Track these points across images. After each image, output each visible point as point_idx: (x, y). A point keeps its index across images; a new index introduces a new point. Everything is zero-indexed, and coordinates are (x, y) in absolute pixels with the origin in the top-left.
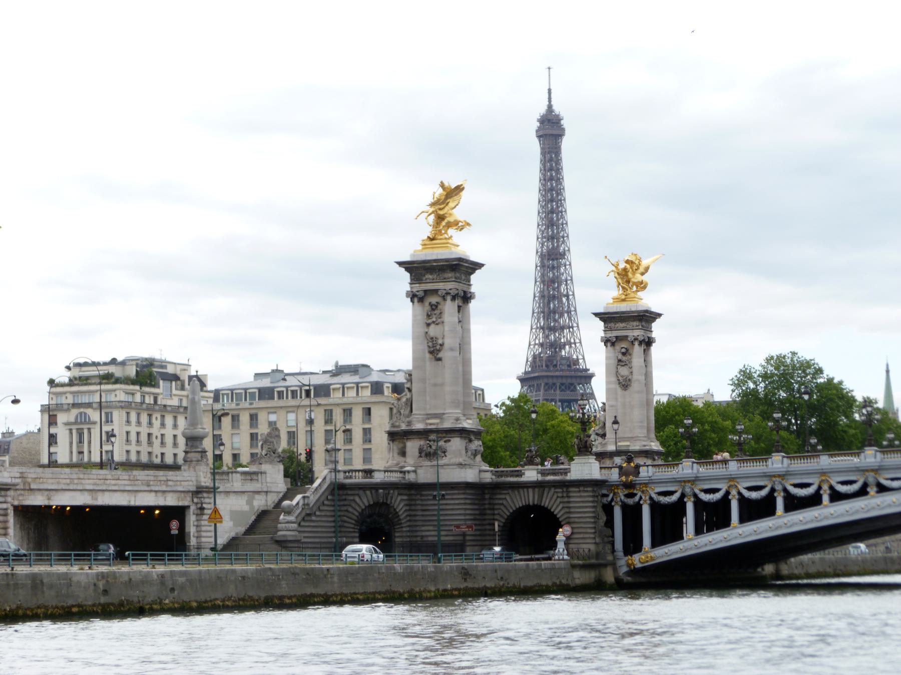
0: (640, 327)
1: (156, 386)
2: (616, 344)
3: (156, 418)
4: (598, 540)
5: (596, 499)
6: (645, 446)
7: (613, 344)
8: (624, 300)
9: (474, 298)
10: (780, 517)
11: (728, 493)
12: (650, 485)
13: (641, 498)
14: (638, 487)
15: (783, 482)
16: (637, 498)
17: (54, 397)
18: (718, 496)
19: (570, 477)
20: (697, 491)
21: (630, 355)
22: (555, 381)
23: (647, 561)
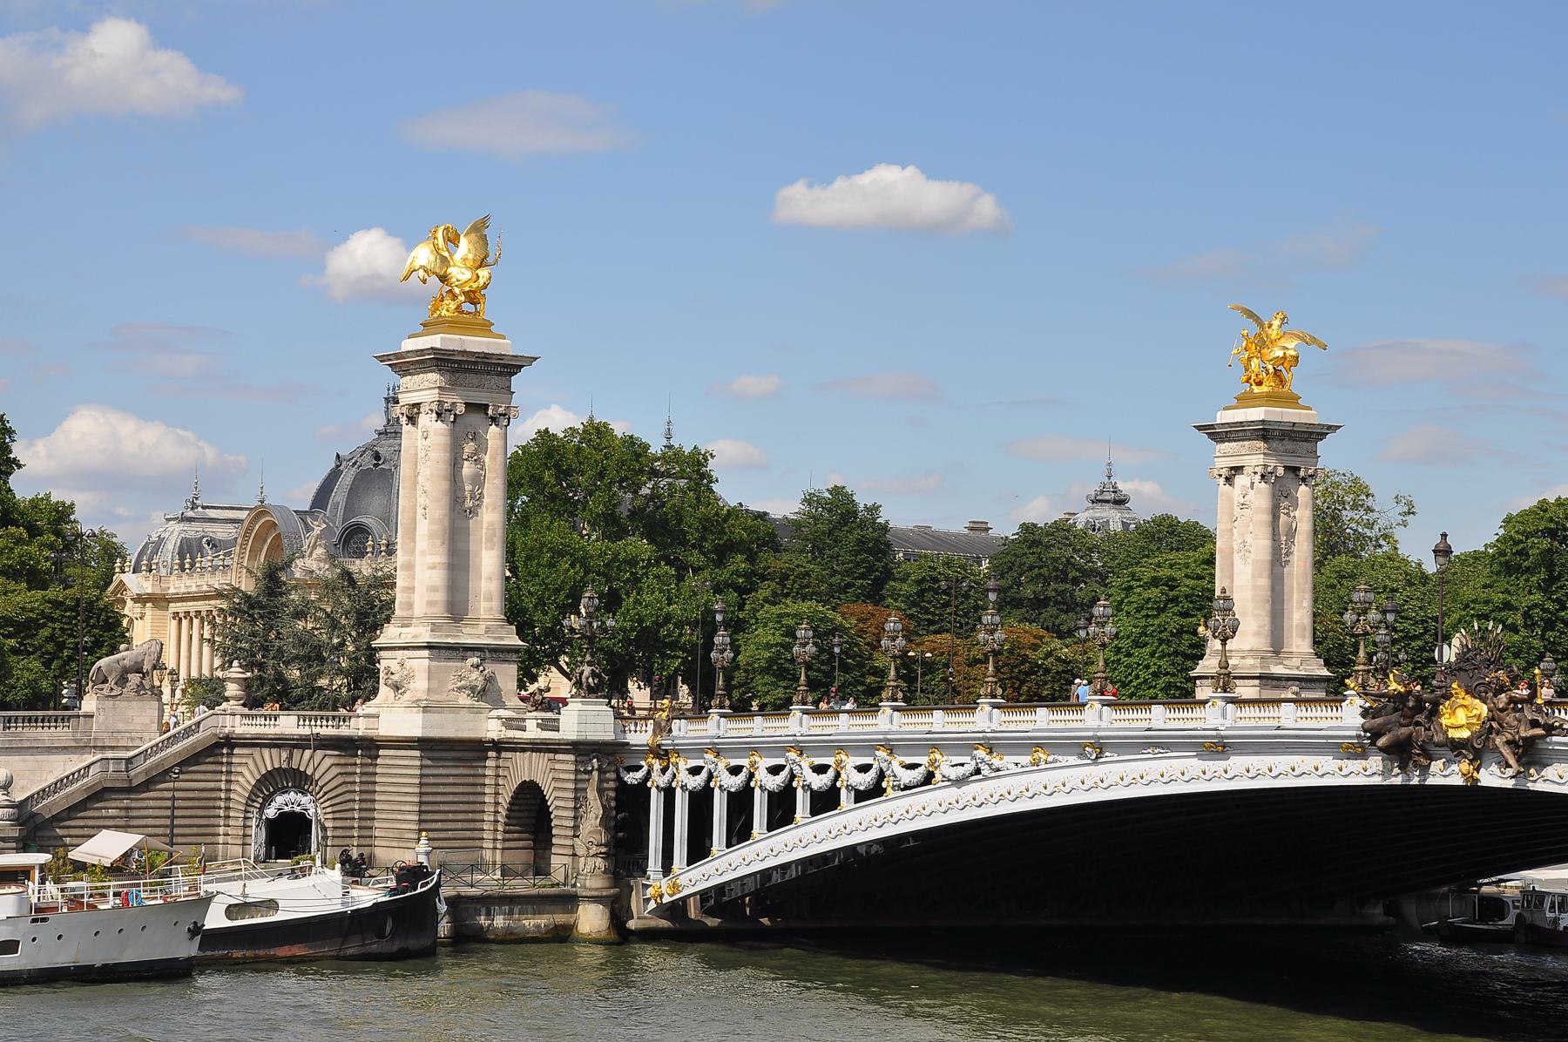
5: (587, 777)
16: (669, 774)
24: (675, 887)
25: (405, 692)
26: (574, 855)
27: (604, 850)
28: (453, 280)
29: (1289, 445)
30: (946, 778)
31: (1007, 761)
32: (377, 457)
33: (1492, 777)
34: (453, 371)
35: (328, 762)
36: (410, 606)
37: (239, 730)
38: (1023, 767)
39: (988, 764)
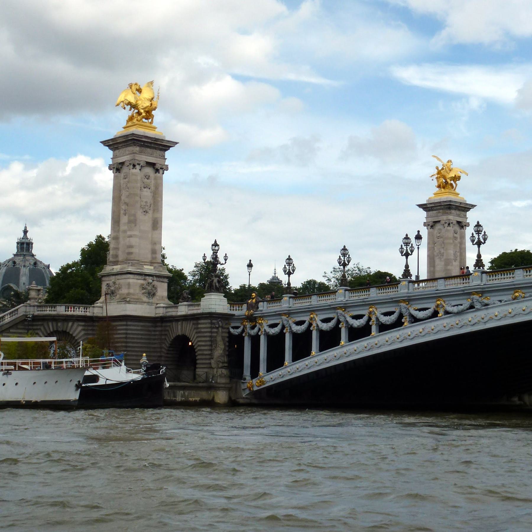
5: (215, 330)
9: (167, 169)
11: (310, 325)
12: (265, 319)
13: (259, 330)
15: (343, 313)
16: (256, 329)
18: (303, 327)
23: (261, 386)
24: (263, 383)
25: (116, 295)
26: (211, 368)
27: (226, 365)
28: (141, 106)
29: (458, 212)
30: (447, 313)
31: (493, 299)
32: (14, 263)
34: (141, 146)
35: (80, 328)
36: (116, 256)
37: (36, 313)
38: (506, 301)
39: (480, 302)
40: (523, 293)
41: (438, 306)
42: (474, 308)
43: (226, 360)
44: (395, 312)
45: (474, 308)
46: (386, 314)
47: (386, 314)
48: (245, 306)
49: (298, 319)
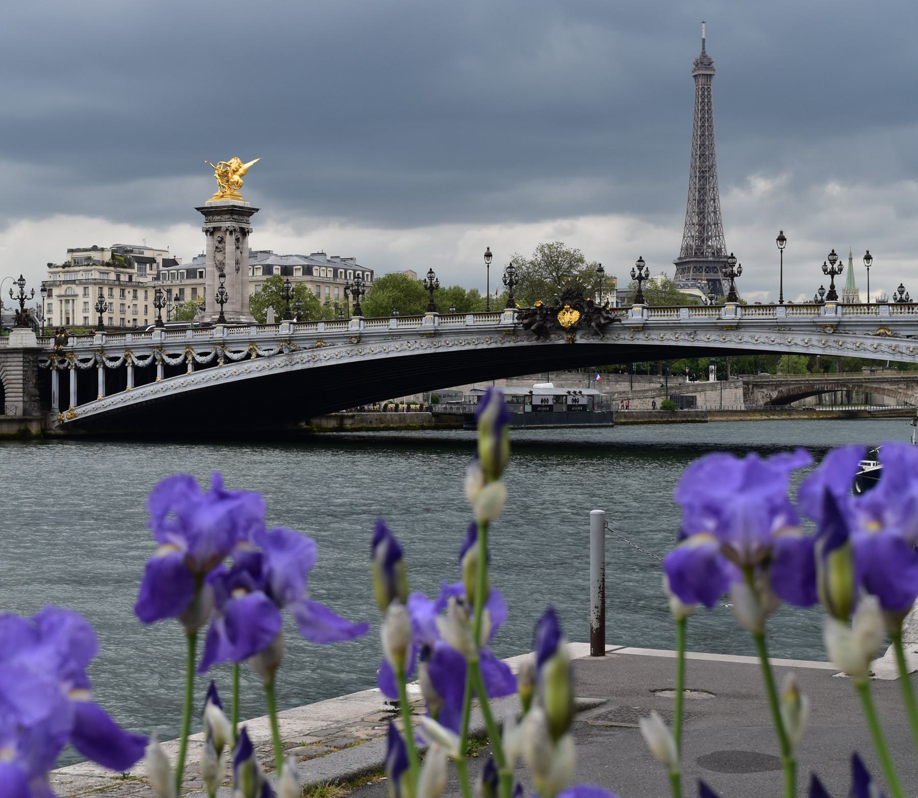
0: (231, 219)
1: (131, 266)
2: (215, 234)
3: (129, 292)
4: (26, 399)
5: (27, 365)
6: (231, 319)
7: (212, 234)
8: (222, 197)
10: (159, 382)
11: (125, 361)
12: (75, 354)
13: (69, 364)
14: (67, 354)
16: (66, 364)
17: (52, 277)
18: (118, 363)
19: (9, 347)
20: (104, 359)
21: (225, 243)
22: (701, 265)
23: (72, 418)
27: (37, 398)
30: (258, 356)
33: (580, 340)
40: (324, 343)
41: (250, 350)
42: (283, 353)
43: (38, 393)
44: (211, 353)
45: (283, 353)
46: (202, 354)
47: (202, 354)
48: (52, 341)
49: (112, 356)
